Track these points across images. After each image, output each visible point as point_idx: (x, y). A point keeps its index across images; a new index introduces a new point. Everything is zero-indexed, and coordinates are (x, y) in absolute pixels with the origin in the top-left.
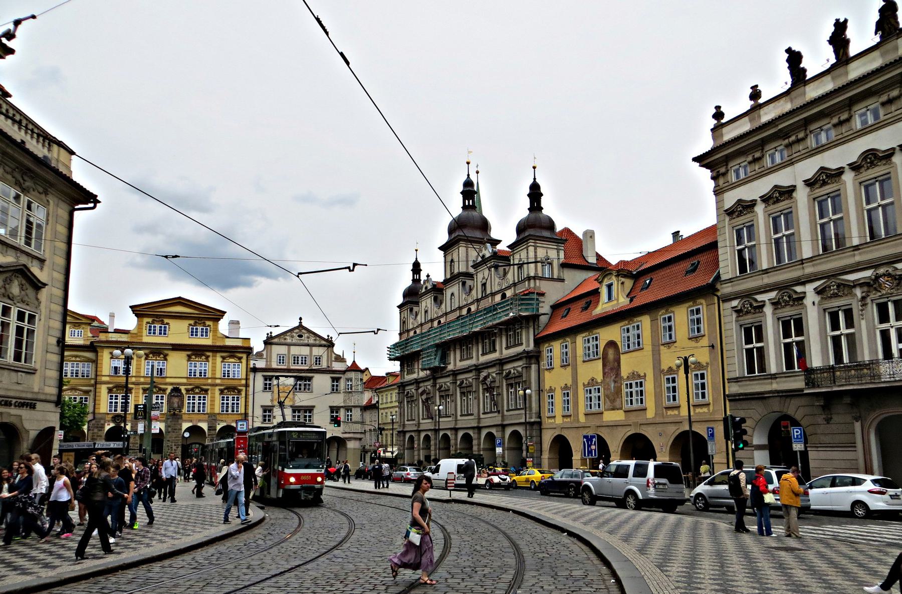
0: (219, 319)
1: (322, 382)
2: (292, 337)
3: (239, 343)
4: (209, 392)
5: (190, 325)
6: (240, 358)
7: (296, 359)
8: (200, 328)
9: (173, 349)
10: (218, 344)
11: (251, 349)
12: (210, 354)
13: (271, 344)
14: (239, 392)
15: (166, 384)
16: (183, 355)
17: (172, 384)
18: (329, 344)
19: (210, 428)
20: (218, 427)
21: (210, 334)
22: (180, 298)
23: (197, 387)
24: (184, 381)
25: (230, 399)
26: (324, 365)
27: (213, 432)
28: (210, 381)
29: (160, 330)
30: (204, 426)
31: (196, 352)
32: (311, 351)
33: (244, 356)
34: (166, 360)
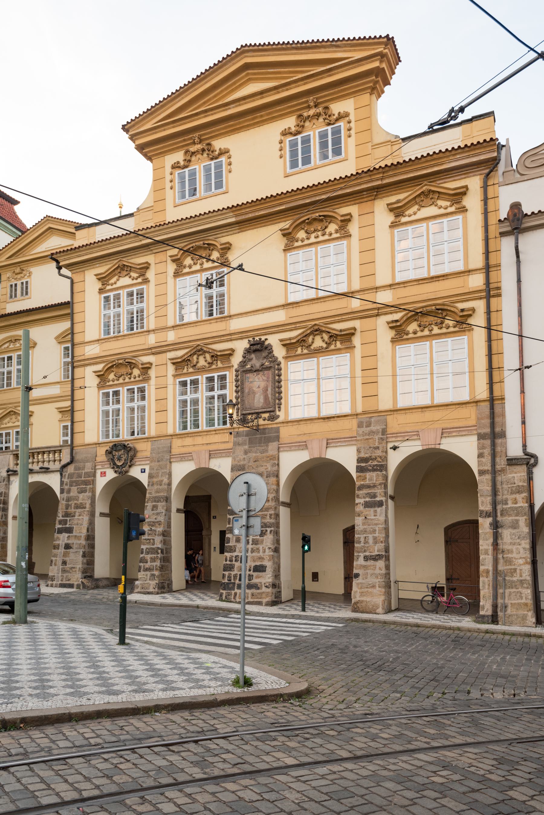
15: (231, 337)
17: (241, 335)
19: (364, 465)
20: (395, 460)
21: (350, 145)
23: (317, 331)
24: (280, 317)
27: (372, 477)
30: (346, 457)
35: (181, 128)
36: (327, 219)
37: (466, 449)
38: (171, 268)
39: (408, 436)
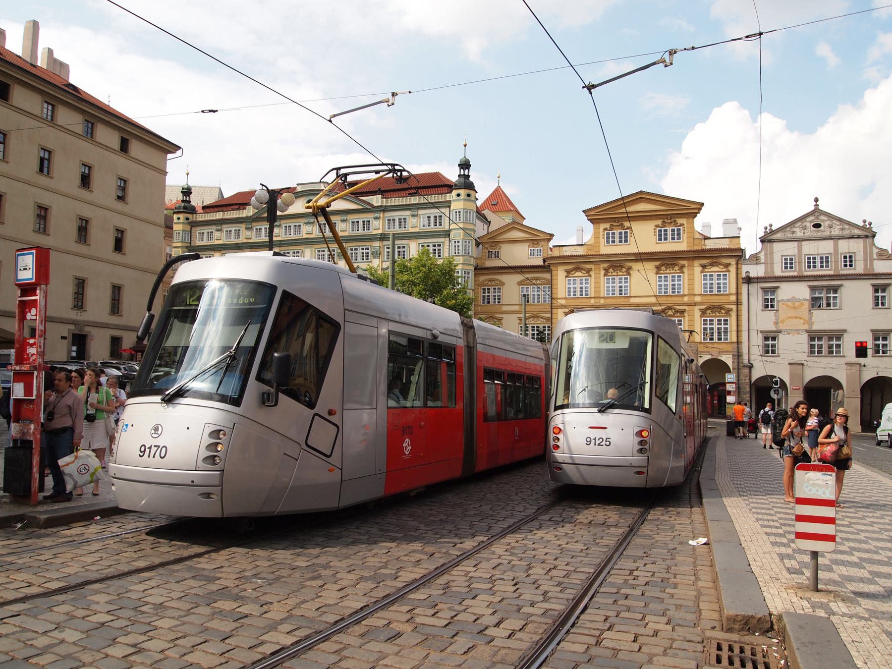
0: (695, 215)
1: (856, 295)
2: (805, 228)
3: (725, 244)
4: (686, 314)
5: (657, 226)
6: (727, 266)
7: (811, 262)
8: (669, 229)
9: (636, 260)
10: (696, 248)
11: (742, 251)
12: (685, 262)
13: (770, 241)
14: (728, 312)
16: (650, 266)
18: (867, 234)
20: (701, 361)
21: (684, 236)
22: (641, 192)
23: (670, 308)
24: (653, 300)
25: (715, 322)
26: (859, 268)
28: (686, 299)
29: (620, 237)
31: (666, 261)
32: (836, 248)
33: (733, 262)
34: (629, 274)
35: (611, 215)
36: (675, 265)
37: (728, 360)
38: (603, 272)
39: (705, 353)
